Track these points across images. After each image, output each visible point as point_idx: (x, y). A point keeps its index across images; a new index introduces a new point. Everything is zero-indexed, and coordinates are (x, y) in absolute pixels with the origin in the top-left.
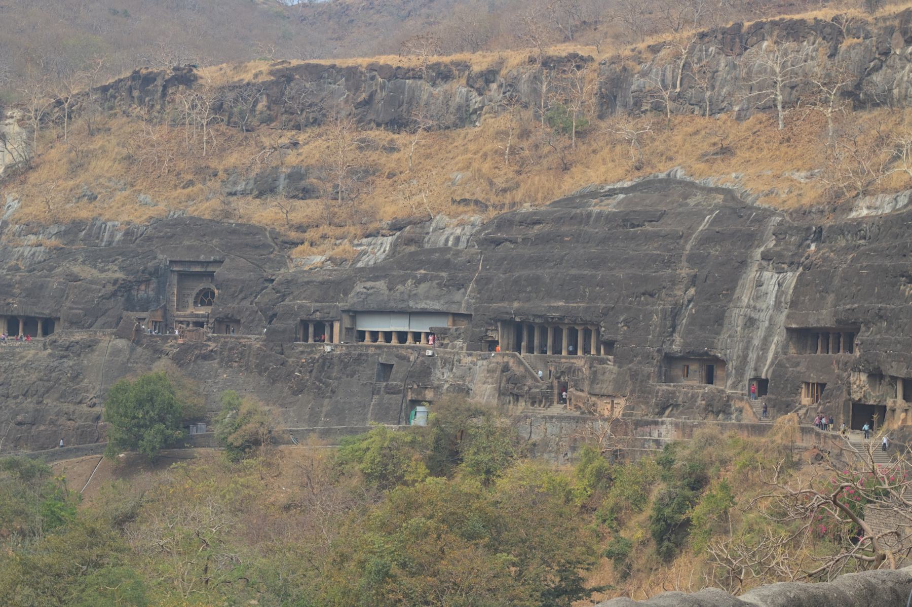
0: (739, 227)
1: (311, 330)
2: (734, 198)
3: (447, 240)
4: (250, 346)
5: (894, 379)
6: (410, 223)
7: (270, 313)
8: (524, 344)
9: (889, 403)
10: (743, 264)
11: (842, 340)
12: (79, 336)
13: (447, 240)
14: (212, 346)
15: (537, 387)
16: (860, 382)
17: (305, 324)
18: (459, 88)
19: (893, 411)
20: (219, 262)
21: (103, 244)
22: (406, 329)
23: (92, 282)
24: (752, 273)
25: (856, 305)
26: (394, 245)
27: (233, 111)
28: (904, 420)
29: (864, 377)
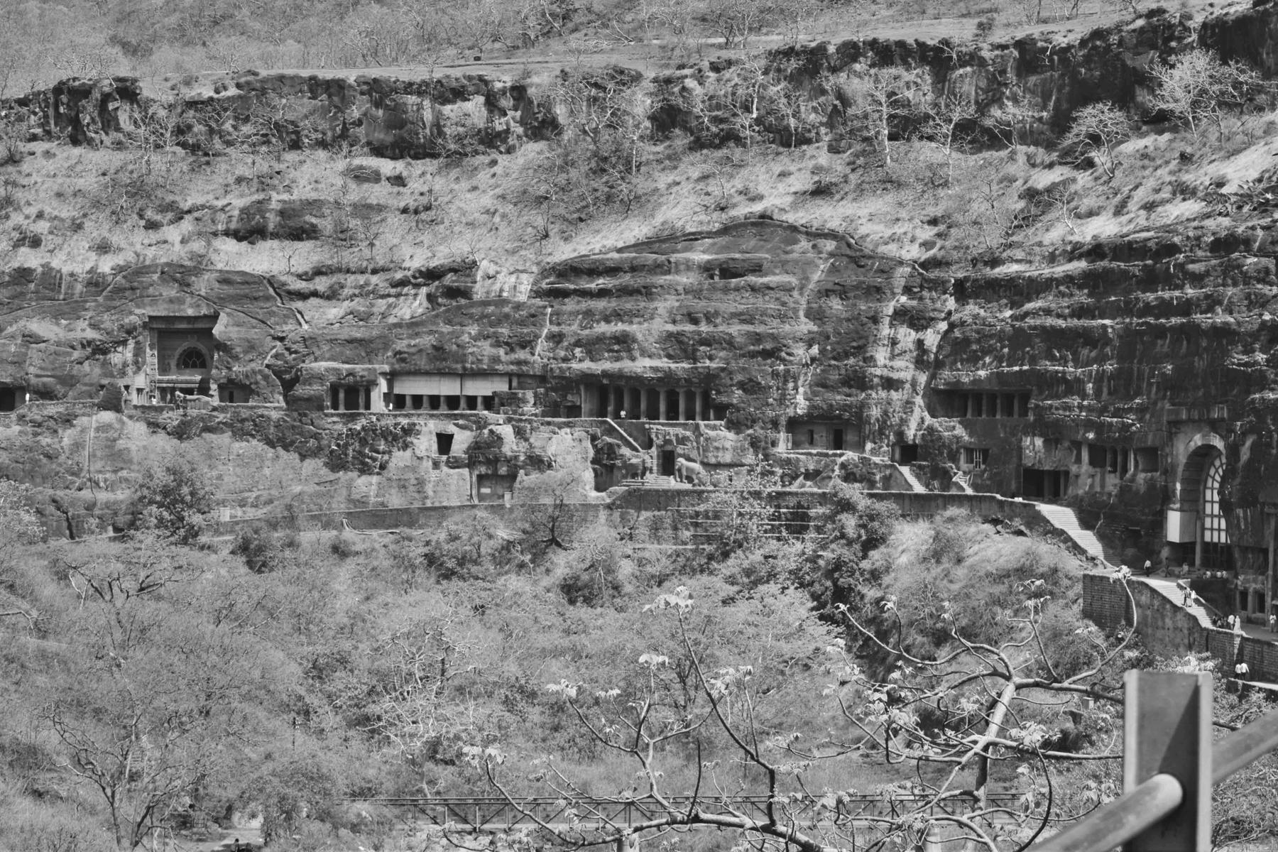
0: (862, 278)
1: (342, 395)
2: (849, 245)
3: (501, 290)
4: (269, 418)
5: (1077, 445)
6: (455, 271)
7: (287, 376)
8: (610, 409)
9: (1074, 469)
10: (875, 320)
11: (998, 401)
12: (53, 409)
13: (501, 290)
14: (221, 417)
15: (637, 457)
16: (1033, 447)
17: (334, 389)
18: (474, 108)
19: (1077, 476)
20: (214, 318)
21: (61, 297)
22: (458, 393)
23: (58, 344)
24: (885, 331)
25: (1025, 368)
26: (430, 297)
27: (197, 130)
28: (1092, 486)
29: (1039, 442)
